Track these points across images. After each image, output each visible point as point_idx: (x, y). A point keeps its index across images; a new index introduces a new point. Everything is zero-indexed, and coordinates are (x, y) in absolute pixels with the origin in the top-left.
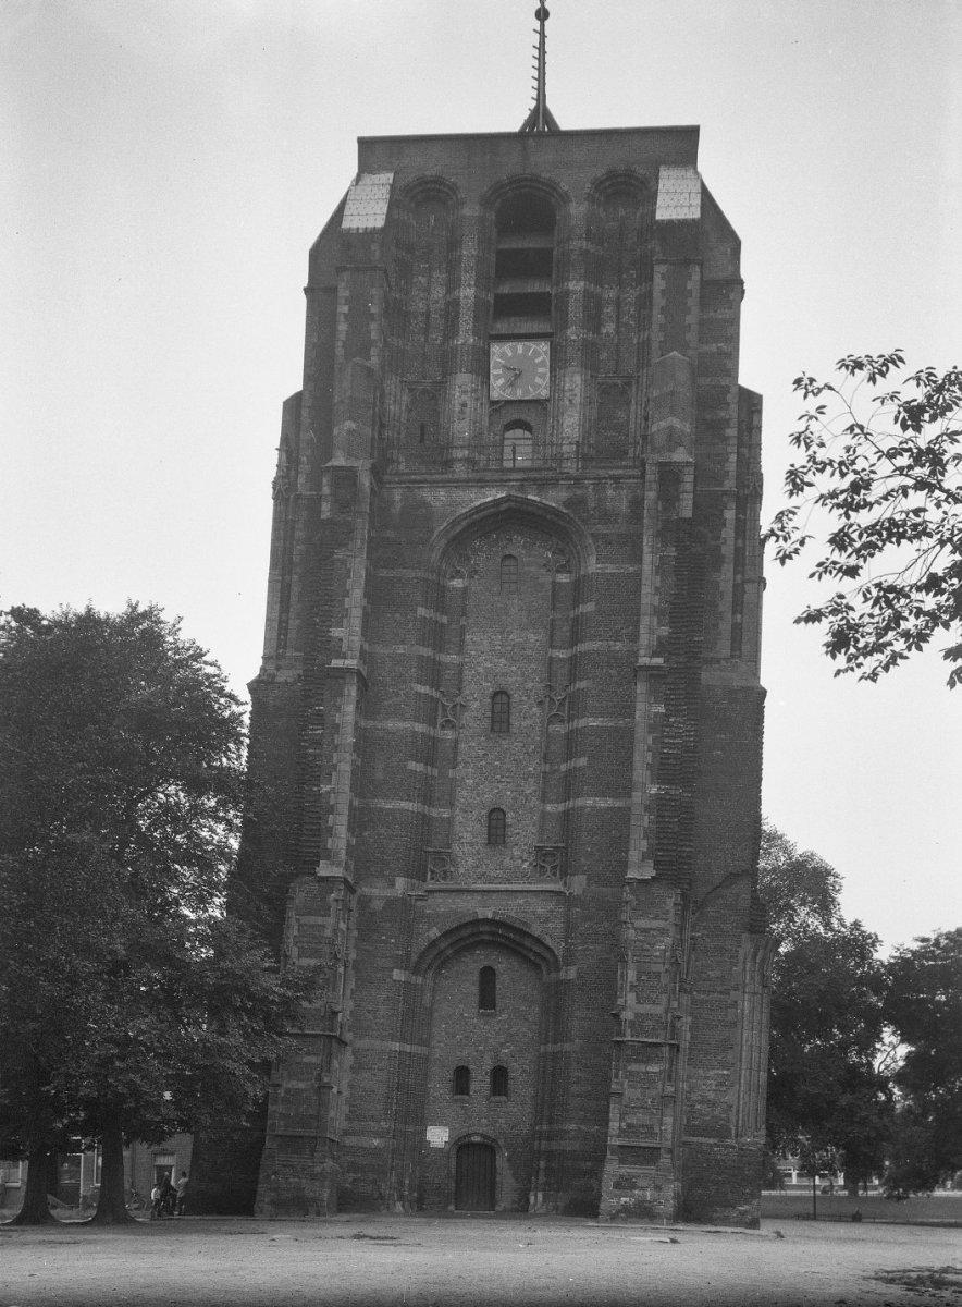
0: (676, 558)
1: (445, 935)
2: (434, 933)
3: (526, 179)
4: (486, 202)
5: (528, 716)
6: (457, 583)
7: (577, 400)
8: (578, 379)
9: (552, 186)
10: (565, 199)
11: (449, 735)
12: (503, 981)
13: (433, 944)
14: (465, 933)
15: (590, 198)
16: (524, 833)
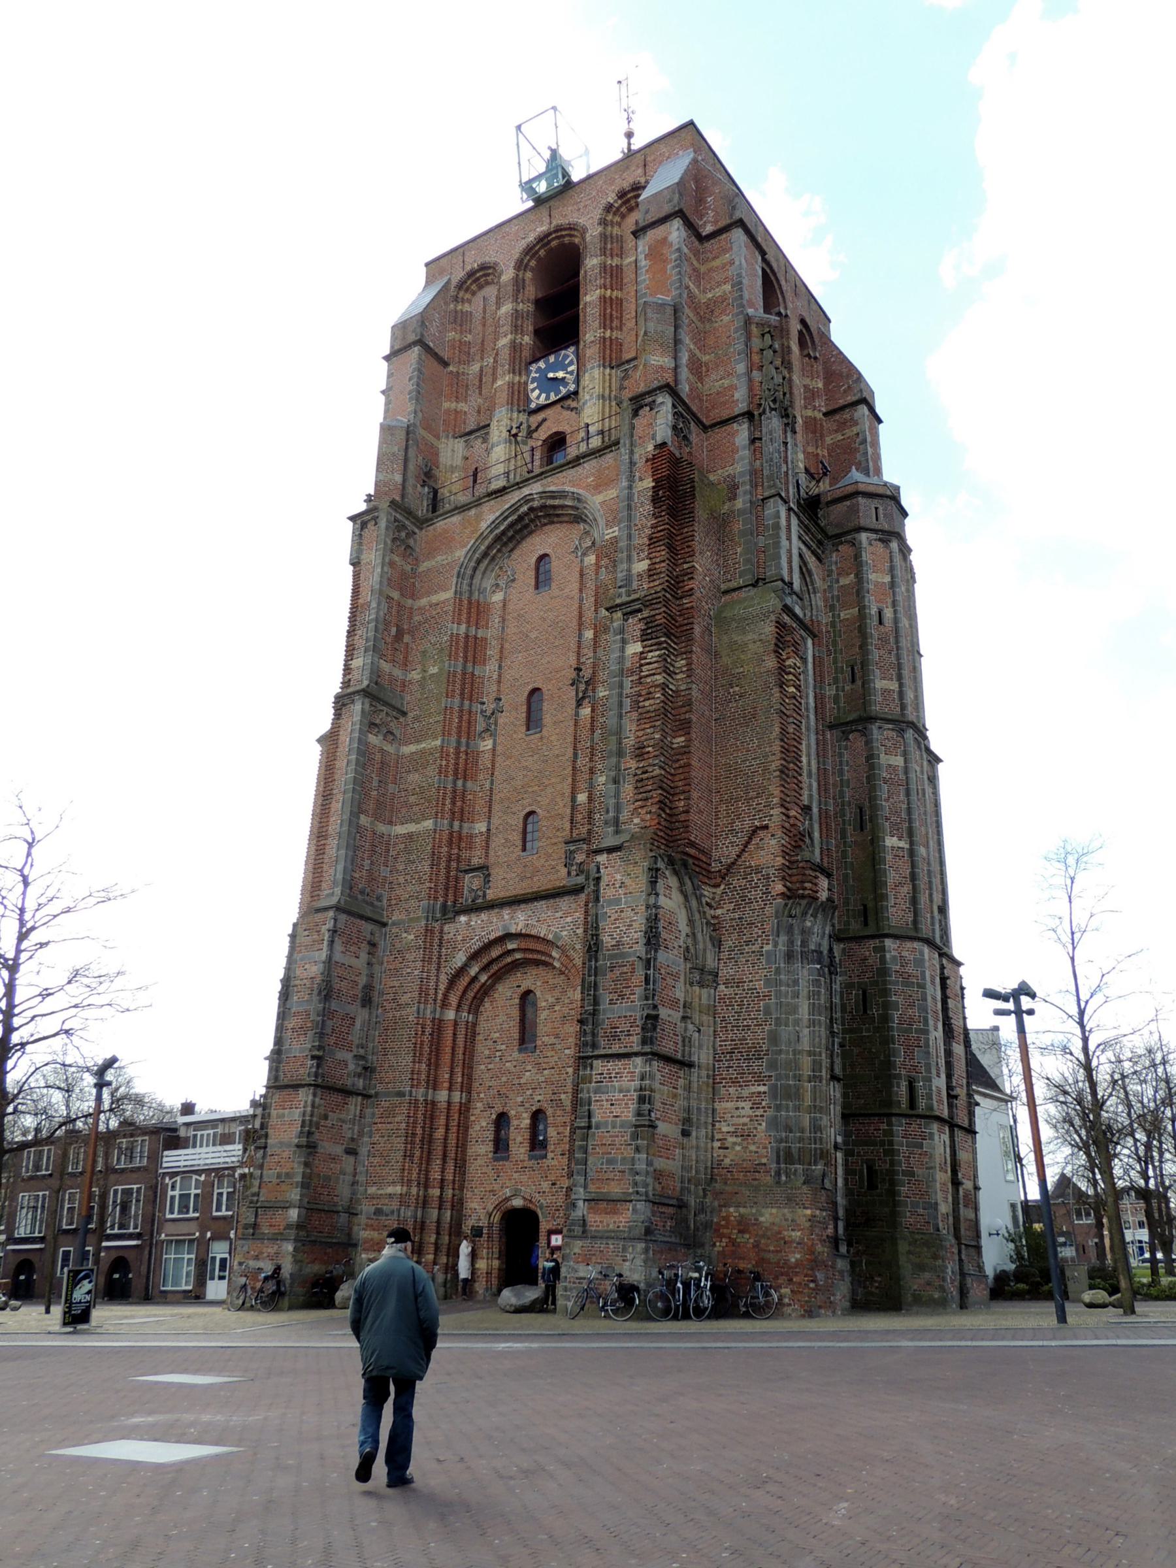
0: (654, 487)
1: (474, 957)
2: (460, 959)
3: (550, 234)
4: (520, 265)
5: (558, 711)
6: (498, 597)
7: (598, 390)
8: (596, 373)
9: (572, 228)
10: (584, 230)
11: (487, 745)
12: (544, 998)
13: (462, 971)
14: (495, 952)
15: (603, 222)
16: (553, 830)
